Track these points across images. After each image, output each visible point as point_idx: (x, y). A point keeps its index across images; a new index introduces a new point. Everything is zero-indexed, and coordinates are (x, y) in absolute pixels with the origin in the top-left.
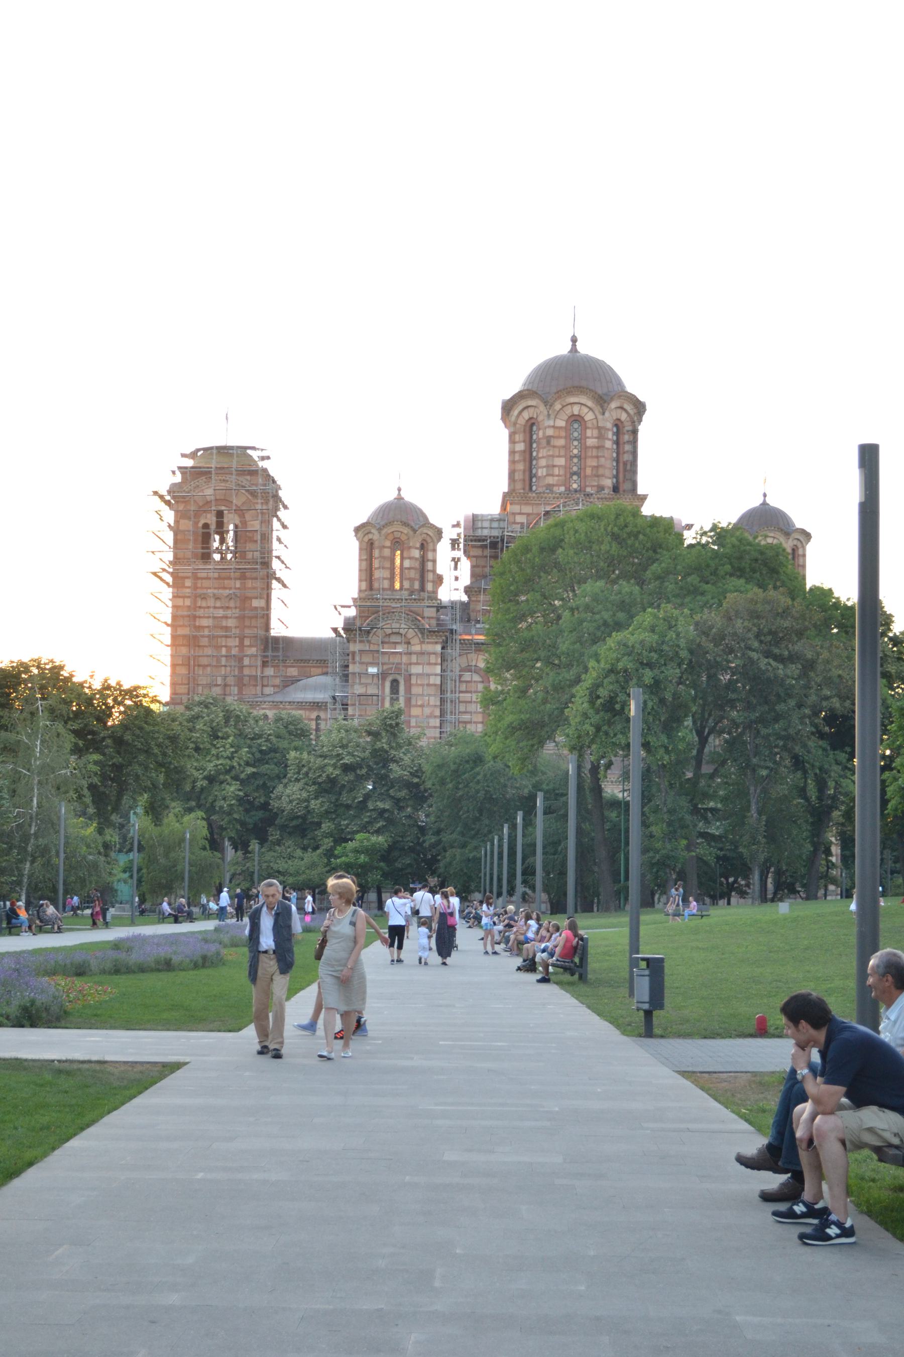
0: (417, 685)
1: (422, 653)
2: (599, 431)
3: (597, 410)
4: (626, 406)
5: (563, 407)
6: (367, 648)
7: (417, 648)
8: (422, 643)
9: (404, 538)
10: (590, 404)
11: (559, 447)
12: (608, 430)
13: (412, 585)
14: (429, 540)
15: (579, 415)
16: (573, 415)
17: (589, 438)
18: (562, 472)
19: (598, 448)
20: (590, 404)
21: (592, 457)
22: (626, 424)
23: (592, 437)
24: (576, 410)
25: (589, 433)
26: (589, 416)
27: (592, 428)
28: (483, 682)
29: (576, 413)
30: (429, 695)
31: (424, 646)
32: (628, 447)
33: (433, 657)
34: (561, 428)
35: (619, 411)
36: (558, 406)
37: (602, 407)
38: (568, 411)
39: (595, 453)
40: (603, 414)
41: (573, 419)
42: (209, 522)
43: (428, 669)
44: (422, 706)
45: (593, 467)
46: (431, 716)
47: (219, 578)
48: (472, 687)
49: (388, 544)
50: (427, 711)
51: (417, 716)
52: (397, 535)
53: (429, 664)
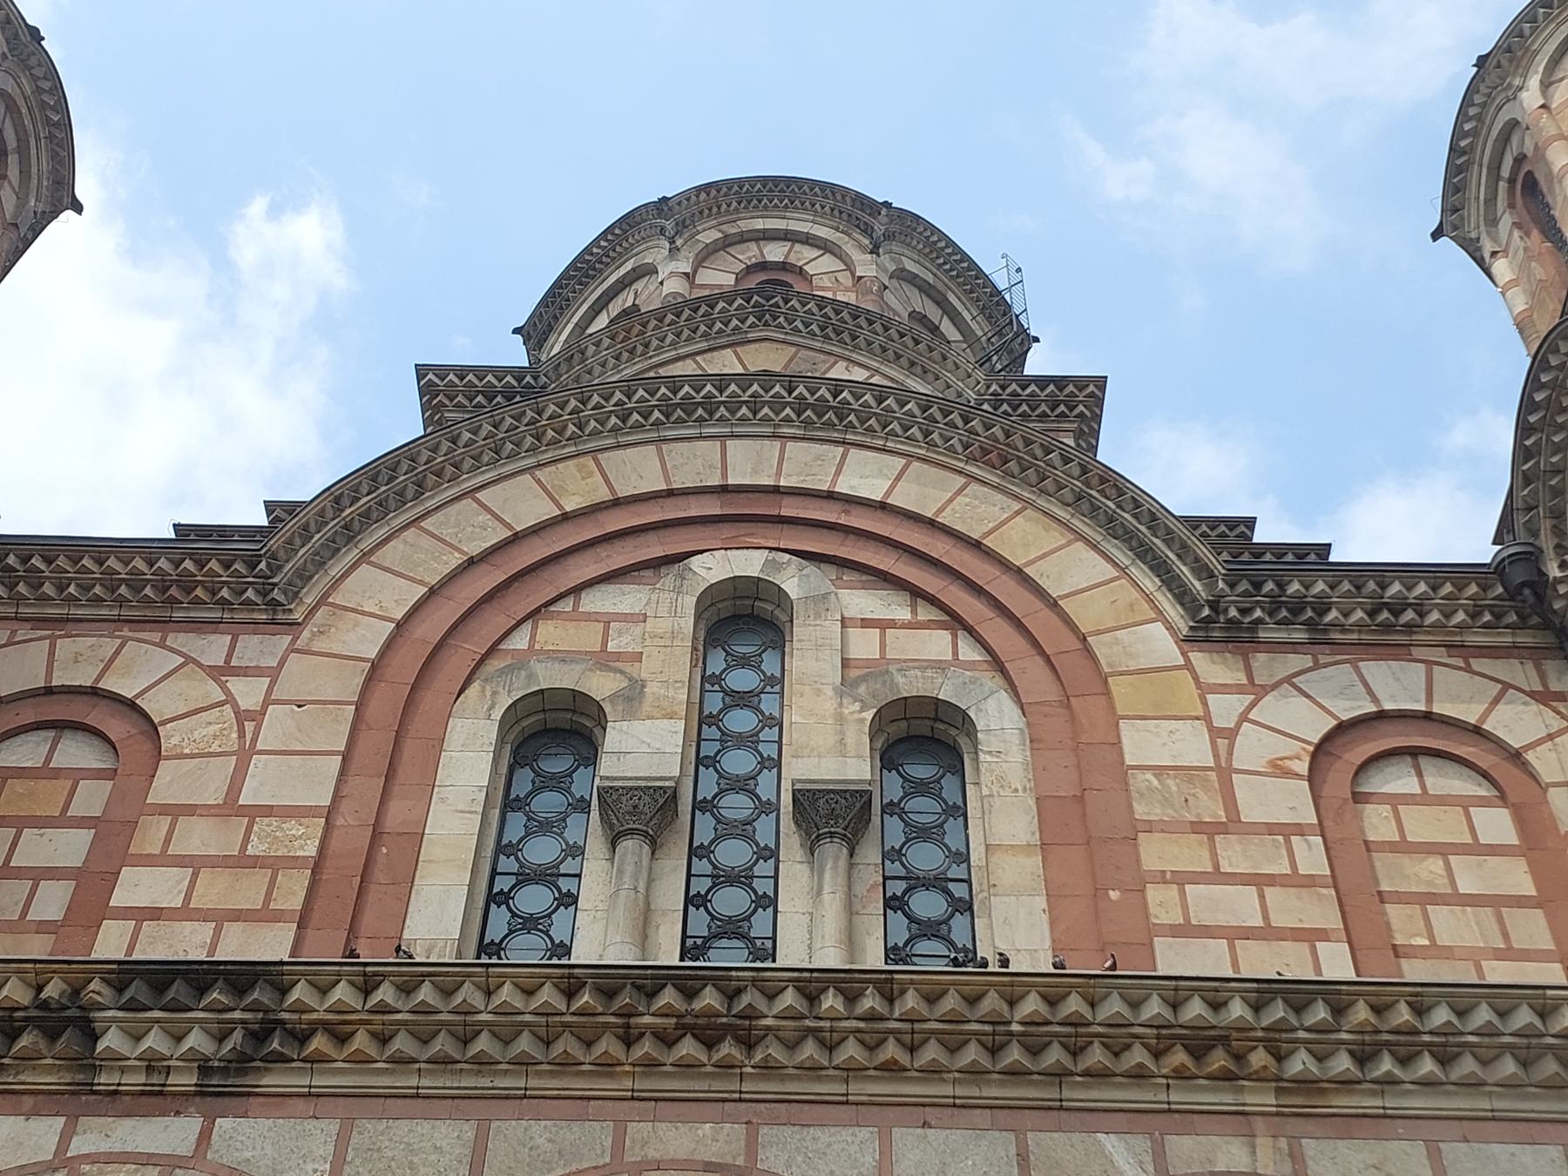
28: (111, 774)
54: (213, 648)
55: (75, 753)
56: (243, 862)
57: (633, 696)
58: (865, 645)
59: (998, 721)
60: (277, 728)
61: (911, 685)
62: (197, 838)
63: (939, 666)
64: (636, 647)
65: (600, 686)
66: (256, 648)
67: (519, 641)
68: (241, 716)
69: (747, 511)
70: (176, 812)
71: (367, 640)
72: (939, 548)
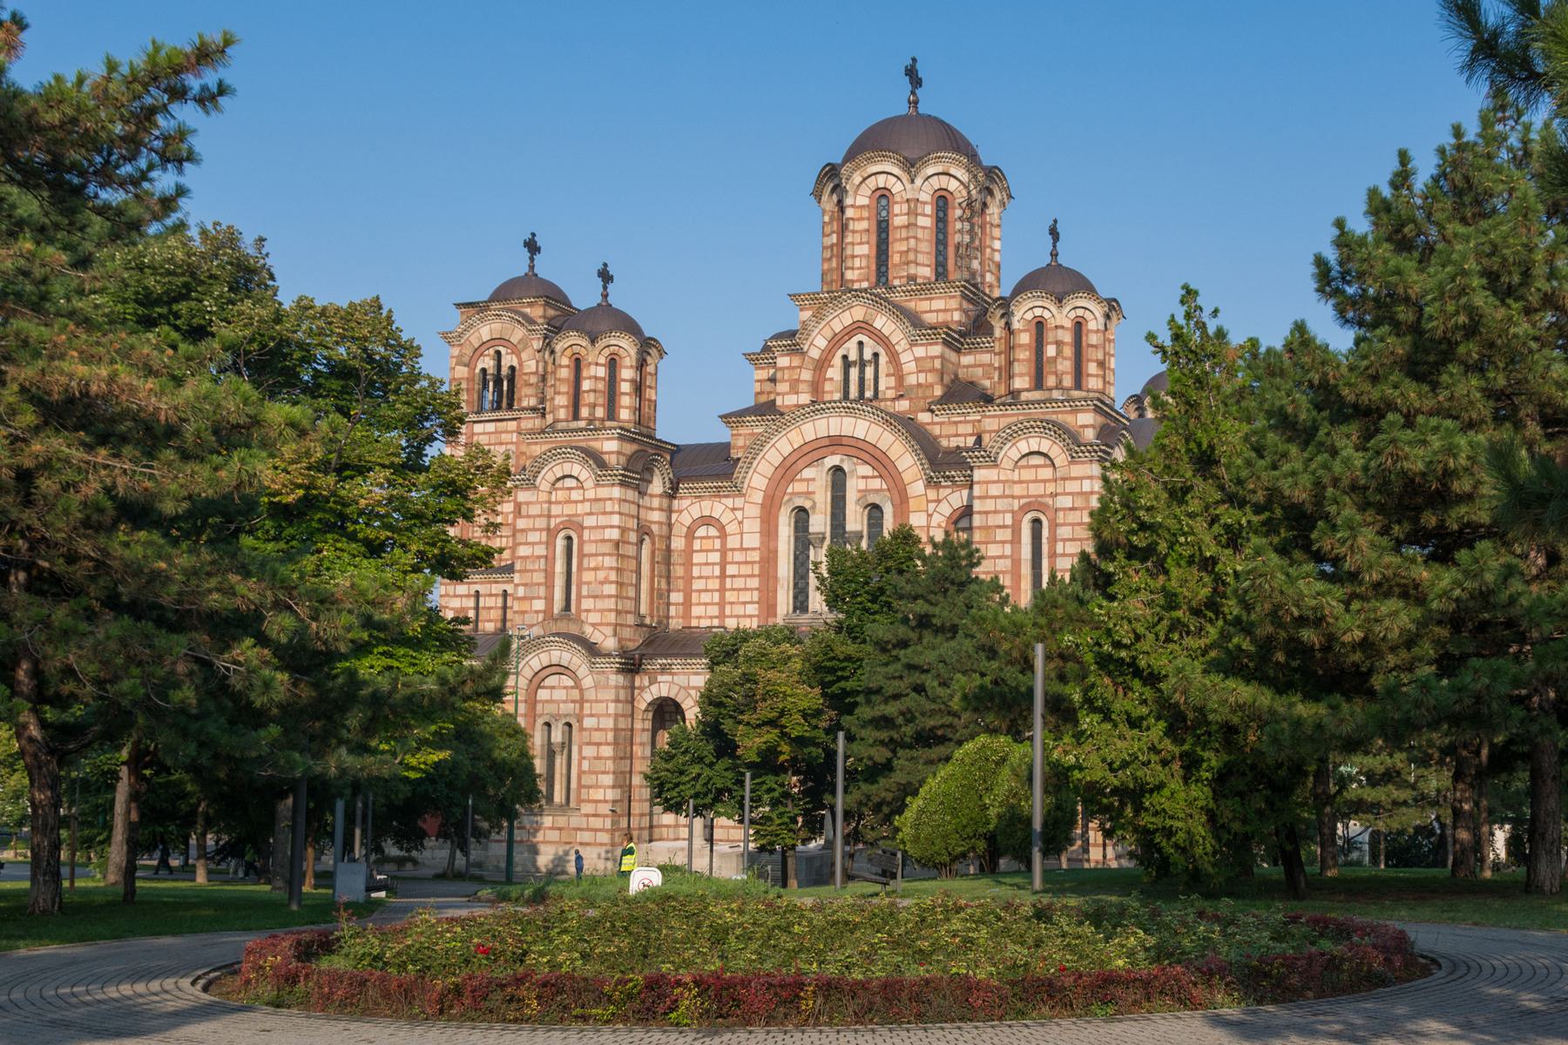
0: (590, 541)
1: (597, 500)
3: (905, 177)
4: (953, 171)
6: (534, 499)
7: (590, 494)
8: (597, 485)
9: (583, 352)
10: (896, 171)
11: (861, 232)
12: (925, 203)
13: (592, 413)
14: (622, 352)
19: (907, 227)
20: (896, 171)
21: (902, 239)
22: (956, 194)
24: (881, 181)
25: (897, 209)
26: (897, 189)
29: (881, 185)
30: (604, 555)
31: (599, 490)
32: (958, 225)
33: (609, 503)
34: (862, 207)
35: (944, 178)
38: (872, 183)
39: (904, 234)
40: (912, 181)
41: (878, 194)
43: (603, 520)
44: (596, 569)
45: (901, 253)
46: (606, 581)
47: (496, 432)
48: (707, 544)
50: (601, 575)
51: (589, 583)
53: (605, 513)
54: (729, 502)
55: (713, 532)
56: (746, 563)
57: (814, 507)
58: (862, 484)
59: (888, 510)
60: (747, 526)
61: (873, 499)
62: (738, 556)
63: (877, 491)
64: (814, 484)
65: (807, 505)
66: (739, 502)
67: (790, 490)
68: (740, 523)
69: (836, 443)
70: (733, 550)
71: (758, 497)
72: (878, 454)
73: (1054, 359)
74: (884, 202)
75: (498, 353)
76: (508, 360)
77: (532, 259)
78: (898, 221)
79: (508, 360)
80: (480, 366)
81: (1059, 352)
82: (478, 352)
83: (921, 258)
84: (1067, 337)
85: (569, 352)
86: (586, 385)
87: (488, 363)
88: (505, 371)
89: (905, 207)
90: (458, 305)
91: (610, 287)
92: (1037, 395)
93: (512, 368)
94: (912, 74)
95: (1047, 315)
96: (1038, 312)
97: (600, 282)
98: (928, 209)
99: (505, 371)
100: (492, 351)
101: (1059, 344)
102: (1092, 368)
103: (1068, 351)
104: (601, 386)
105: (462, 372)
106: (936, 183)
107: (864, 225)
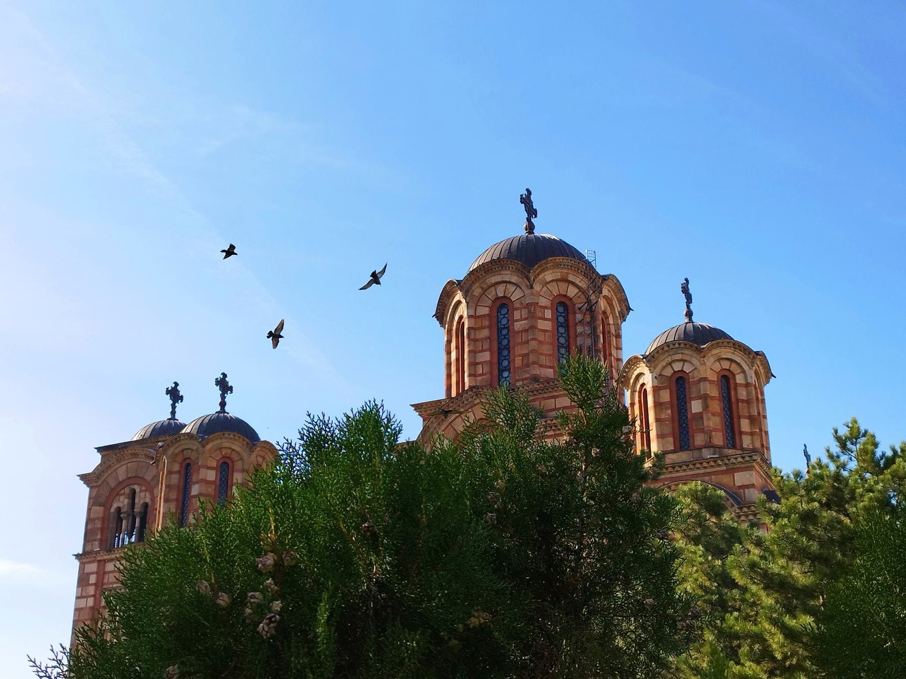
2: (530, 312)
3: (524, 283)
4: (571, 278)
5: (484, 291)
9: (193, 456)
10: (514, 279)
11: (482, 340)
14: (235, 456)
15: (504, 297)
16: (498, 298)
17: (517, 321)
18: (487, 369)
20: (514, 279)
21: (522, 343)
23: (522, 319)
25: (517, 315)
27: (520, 309)
29: (501, 294)
32: (579, 329)
35: (563, 285)
36: (477, 291)
37: (528, 279)
38: (491, 294)
40: (532, 287)
41: (498, 304)
42: (121, 505)
49: (176, 467)
52: (187, 454)
73: (699, 416)
74: (504, 311)
75: (133, 493)
76: (142, 498)
77: (174, 407)
78: (518, 326)
79: (142, 498)
80: (115, 506)
81: (706, 407)
82: (114, 493)
83: (543, 360)
84: (713, 391)
85: (180, 459)
86: (195, 490)
87: (123, 502)
88: (137, 509)
89: (525, 313)
90: (99, 449)
91: (229, 397)
92: (683, 456)
93: (146, 506)
94: (526, 200)
95: (687, 368)
96: (677, 367)
97: (217, 391)
98: (548, 314)
99: (137, 509)
100: (127, 490)
101: (705, 398)
102: (745, 425)
103: (716, 406)
104: (211, 490)
105: (99, 511)
106: (555, 289)
107: (485, 333)
